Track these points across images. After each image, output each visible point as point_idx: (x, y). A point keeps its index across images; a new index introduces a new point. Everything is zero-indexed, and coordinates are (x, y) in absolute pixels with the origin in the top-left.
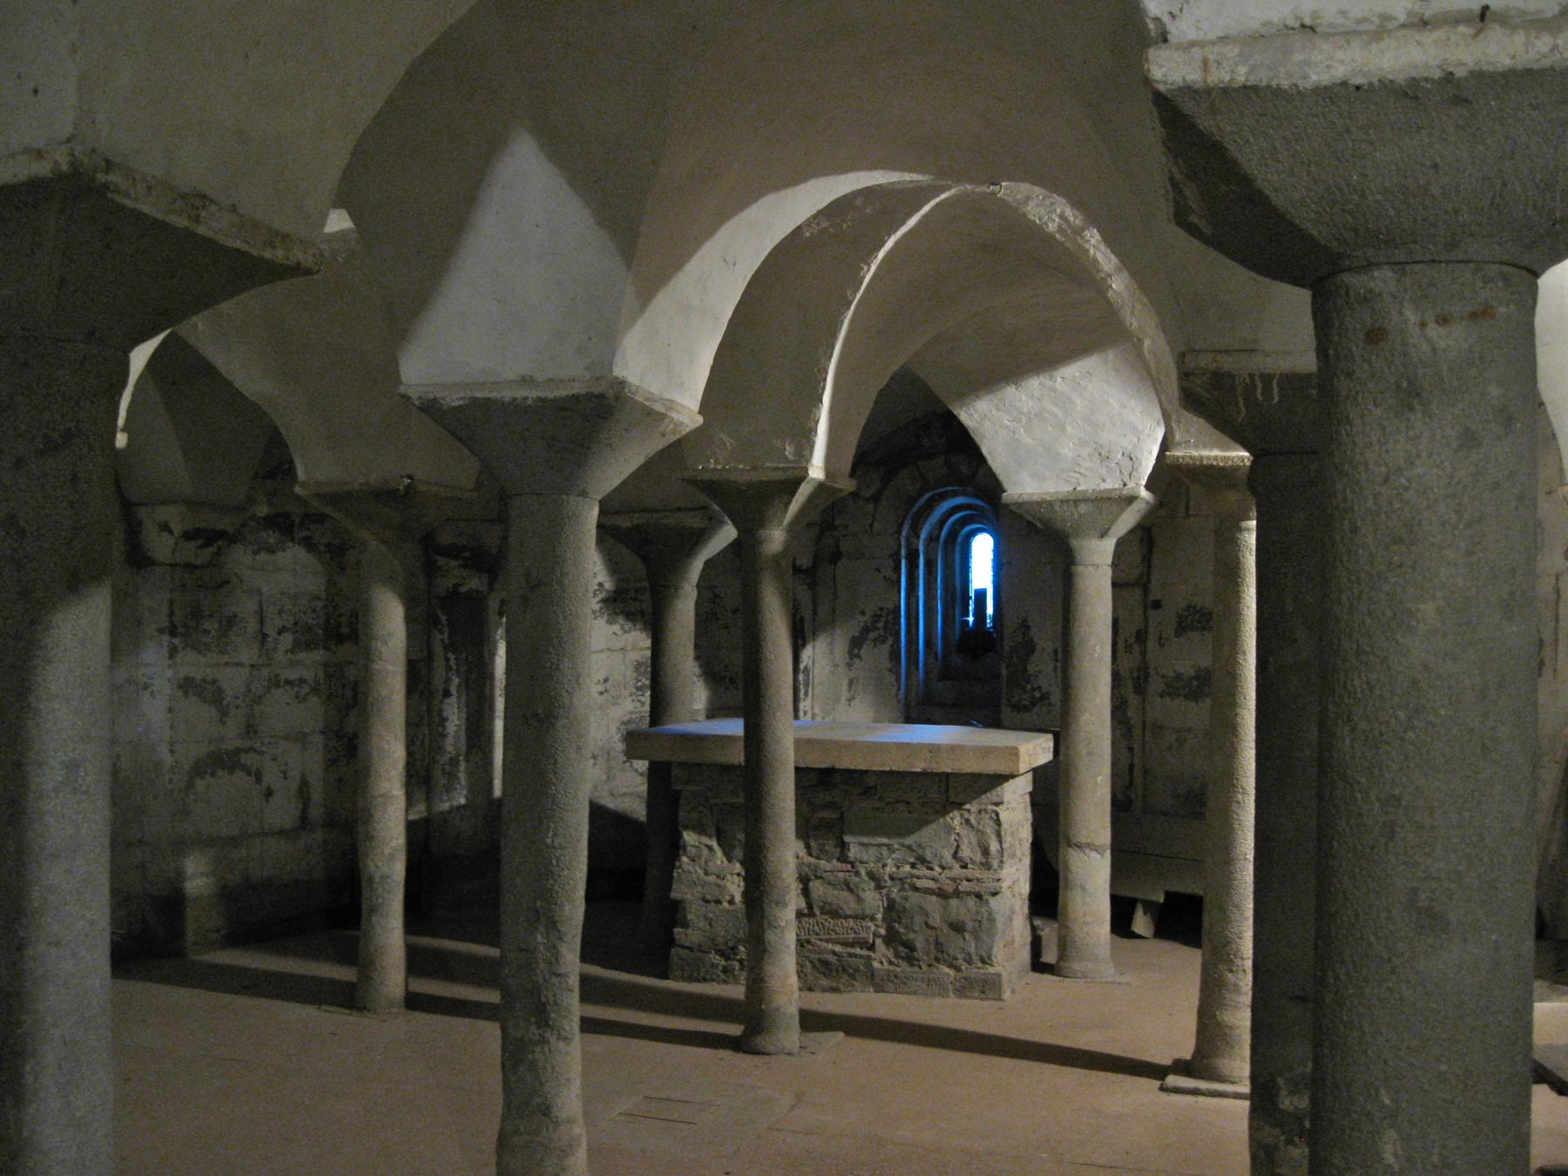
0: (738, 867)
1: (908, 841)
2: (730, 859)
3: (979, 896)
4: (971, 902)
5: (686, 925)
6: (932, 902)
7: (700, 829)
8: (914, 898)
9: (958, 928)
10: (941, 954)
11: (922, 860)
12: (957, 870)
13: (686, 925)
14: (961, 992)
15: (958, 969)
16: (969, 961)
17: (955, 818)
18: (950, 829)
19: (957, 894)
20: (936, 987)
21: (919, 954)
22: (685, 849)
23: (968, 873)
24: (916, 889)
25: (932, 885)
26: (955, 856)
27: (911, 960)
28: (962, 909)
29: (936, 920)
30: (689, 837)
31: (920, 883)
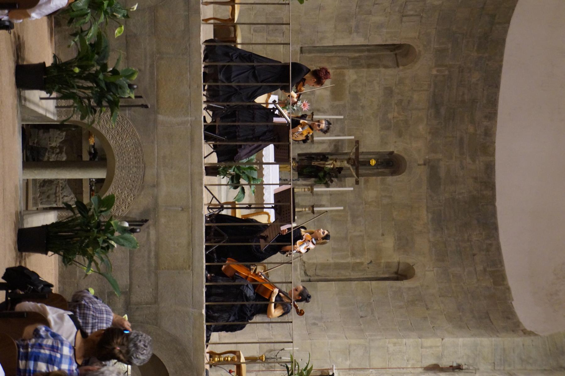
0: (58, 145)
1: (67, 186)
2: (61, 143)
3: (56, 201)
4: (54, 200)
5: (44, 133)
6: (54, 191)
7: (66, 135)
8: (54, 187)
9: (48, 197)
10: (42, 193)
11: (63, 189)
12: (61, 197)
13: (44, 133)
14: (34, 198)
15: (39, 197)
16: (41, 200)
17: (73, 196)
18: (70, 195)
19: (56, 197)
20: (34, 193)
21: (42, 188)
22: (62, 132)
23: (61, 199)
24: (56, 187)
25: (58, 191)
26: (64, 196)
27: (40, 186)
28: (52, 198)
29: (50, 192)
30: (64, 133)
31: (58, 189)
